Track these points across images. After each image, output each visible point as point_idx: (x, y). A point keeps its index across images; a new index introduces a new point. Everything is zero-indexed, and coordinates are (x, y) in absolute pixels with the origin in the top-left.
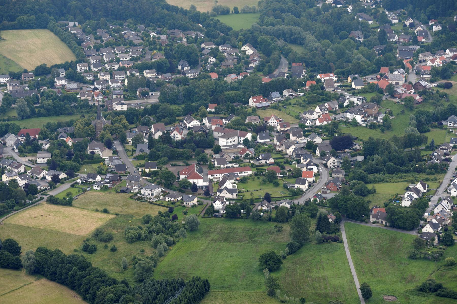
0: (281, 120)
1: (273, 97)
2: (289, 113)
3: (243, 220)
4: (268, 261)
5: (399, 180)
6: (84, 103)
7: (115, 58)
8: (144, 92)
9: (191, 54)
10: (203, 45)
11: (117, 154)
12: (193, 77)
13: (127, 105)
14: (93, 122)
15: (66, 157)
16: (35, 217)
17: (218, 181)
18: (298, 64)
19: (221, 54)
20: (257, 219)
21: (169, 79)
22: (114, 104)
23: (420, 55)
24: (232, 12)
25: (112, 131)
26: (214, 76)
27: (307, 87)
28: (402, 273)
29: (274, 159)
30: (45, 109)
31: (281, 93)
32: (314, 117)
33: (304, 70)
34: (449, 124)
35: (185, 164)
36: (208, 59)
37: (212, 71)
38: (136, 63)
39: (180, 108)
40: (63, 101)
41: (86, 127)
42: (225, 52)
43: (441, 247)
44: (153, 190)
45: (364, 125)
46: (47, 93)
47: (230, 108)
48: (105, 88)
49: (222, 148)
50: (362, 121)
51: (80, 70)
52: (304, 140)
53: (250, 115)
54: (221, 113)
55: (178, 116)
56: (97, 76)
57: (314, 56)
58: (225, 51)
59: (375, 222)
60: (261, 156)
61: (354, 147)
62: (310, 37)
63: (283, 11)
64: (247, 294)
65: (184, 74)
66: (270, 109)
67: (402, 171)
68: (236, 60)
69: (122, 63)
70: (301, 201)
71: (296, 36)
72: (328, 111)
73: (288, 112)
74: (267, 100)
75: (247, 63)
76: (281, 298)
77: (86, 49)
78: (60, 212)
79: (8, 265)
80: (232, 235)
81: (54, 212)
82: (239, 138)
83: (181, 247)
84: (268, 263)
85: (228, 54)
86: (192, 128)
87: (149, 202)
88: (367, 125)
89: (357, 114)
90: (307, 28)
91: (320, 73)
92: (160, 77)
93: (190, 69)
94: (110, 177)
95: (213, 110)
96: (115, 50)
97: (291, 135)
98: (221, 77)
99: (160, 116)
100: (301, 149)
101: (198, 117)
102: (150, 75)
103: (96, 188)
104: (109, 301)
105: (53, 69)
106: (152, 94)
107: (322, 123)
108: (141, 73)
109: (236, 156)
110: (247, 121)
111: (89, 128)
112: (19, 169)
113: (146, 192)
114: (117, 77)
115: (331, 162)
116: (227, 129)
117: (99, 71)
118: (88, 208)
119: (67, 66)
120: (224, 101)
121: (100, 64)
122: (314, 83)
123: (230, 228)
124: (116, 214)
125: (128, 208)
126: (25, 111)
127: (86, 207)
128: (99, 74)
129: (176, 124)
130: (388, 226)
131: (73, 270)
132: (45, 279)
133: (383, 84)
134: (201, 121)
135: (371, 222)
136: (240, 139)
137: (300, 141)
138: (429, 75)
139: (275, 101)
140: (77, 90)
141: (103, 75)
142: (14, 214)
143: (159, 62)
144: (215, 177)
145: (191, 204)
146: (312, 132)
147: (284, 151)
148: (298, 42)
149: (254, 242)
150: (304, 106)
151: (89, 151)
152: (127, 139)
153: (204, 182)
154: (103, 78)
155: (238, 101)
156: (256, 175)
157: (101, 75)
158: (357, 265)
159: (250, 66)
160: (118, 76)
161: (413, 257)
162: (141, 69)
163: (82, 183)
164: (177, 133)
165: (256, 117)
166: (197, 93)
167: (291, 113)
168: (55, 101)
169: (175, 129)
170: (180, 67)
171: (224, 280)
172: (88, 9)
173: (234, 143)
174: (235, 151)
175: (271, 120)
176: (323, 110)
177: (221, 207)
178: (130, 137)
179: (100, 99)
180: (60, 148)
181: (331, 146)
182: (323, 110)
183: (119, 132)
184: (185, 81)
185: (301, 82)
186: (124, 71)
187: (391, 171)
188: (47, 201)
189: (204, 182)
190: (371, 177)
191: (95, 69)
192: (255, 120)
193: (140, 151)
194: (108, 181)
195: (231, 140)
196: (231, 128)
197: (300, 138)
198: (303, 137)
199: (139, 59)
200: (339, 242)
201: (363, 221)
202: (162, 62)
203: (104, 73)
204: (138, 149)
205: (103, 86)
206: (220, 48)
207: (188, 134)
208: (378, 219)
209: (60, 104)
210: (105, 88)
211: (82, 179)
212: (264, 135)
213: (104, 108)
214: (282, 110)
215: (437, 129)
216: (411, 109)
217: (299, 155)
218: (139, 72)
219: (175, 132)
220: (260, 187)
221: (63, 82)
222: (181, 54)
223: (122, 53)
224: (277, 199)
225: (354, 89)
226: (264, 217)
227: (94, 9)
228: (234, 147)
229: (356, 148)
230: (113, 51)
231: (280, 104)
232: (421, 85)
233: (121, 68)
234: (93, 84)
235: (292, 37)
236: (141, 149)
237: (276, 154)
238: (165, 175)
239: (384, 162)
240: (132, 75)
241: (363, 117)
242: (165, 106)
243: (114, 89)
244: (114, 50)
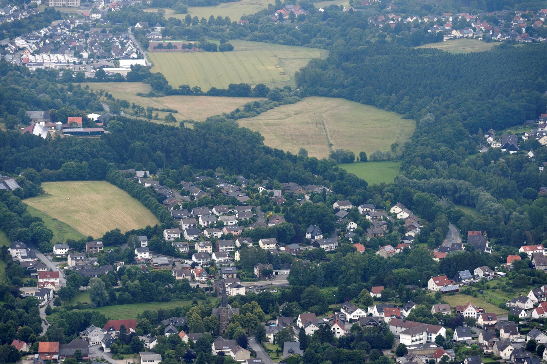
0: (481, 310)
1: (462, 277)
2: (490, 300)
6: (183, 285)
7: (215, 222)
8: (266, 269)
9: (324, 217)
10: (336, 205)
11: (255, 356)
12: (329, 250)
13: (244, 288)
14: (214, 310)
15: (184, 359)
18: (476, 233)
19: (363, 217)
21: (296, 252)
22: (226, 286)
24: (358, 159)
25: (243, 323)
26: (361, 248)
27: (509, 264)
30: (129, 293)
31: (472, 273)
32: (527, 307)
33: (488, 242)
36: (347, 224)
37: (356, 241)
38: (246, 229)
39: (330, 292)
40: (153, 281)
41: (206, 317)
42: (368, 215)
46: (129, 269)
47: (405, 292)
48: (208, 265)
49: (408, 348)
51: (169, 239)
52: (521, 338)
53: (433, 303)
54: (389, 300)
55: (330, 303)
56: (194, 247)
57: (497, 221)
58: (368, 213)
60: (466, 360)
62: (485, 195)
63: (435, 158)
65: (317, 244)
66: (460, 295)
68: (386, 226)
69: (227, 229)
71: (462, 193)
72: (545, 298)
73: (487, 298)
74: (454, 282)
75: (403, 231)
77: (172, 208)
82: (428, 335)
85: (373, 217)
86: (355, 320)
90: (478, 182)
91: (523, 245)
92: (282, 249)
93: (324, 238)
95: (379, 296)
96: (214, 210)
97: (502, 332)
98: (370, 250)
99: (304, 303)
100: (523, 350)
101: (361, 305)
102: (268, 246)
105: (131, 236)
106: (277, 273)
107: (541, 315)
108: (256, 243)
110: (433, 311)
111: (210, 318)
114: (222, 248)
116: (410, 322)
117: (195, 240)
119: (149, 233)
120: (392, 284)
121: (196, 230)
122: (519, 258)
126: (102, 295)
128: (196, 244)
129: (330, 314)
134: (366, 311)
136: (429, 336)
137: (515, 340)
139: (464, 284)
140: (167, 267)
141: (203, 245)
143: (280, 228)
146: (533, 328)
147: (496, 354)
148: (465, 202)
150: (510, 291)
151: (215, 352)
152: (267, 334)
154: (203, 249)
155: (412, 283)
157: (200, 245)
159: (407, 235)
160: (224, 248)
162: (256, 237)
164: (339, 327)
165: (446, 305)
166: (342, 272)
167: (492, 301)
168: (144, 282)
169: (334, 320)
170: (308, 236)
172: (159, 153)
173: (421, 342)
174: (426, 352)
175: (467, 309)
176: (539, 297)
178: (270, 332)
180: (174, 346)
182: (539, 297)
184: (320, 255)
185: (497, 257)
186: (231, 240)
191: (189, 238)
192: (445, 310)
193: (289, 352)
195: (417, 337)
196: (415, 320)
197: (514, 336)
198: (519, 335)
199: (250, 223)
202: (285, 228)
203: (204, 243)
206: (360, 209)
207: (352, 329)
209: (150, 285)
210: (208, 265)
212: (464, 330)
213: (212, 292)
214: (478, 296)
217: (521, 359)
218: (254, 241)
219: (336, 326)
221: (147, 255)
222: (310, 217)
223: (224, 215)
227: (167, 152)
228: (424, 347)
230: (210, 212)
231: (473, 288)
233: (227, 236)
234: (190, 258)
235: (457, 195)
236: (291, 349)
237: (485, 357)
240: (244, 246)
242: (312, 289)
243: (221, 266)
244: (212, 211)
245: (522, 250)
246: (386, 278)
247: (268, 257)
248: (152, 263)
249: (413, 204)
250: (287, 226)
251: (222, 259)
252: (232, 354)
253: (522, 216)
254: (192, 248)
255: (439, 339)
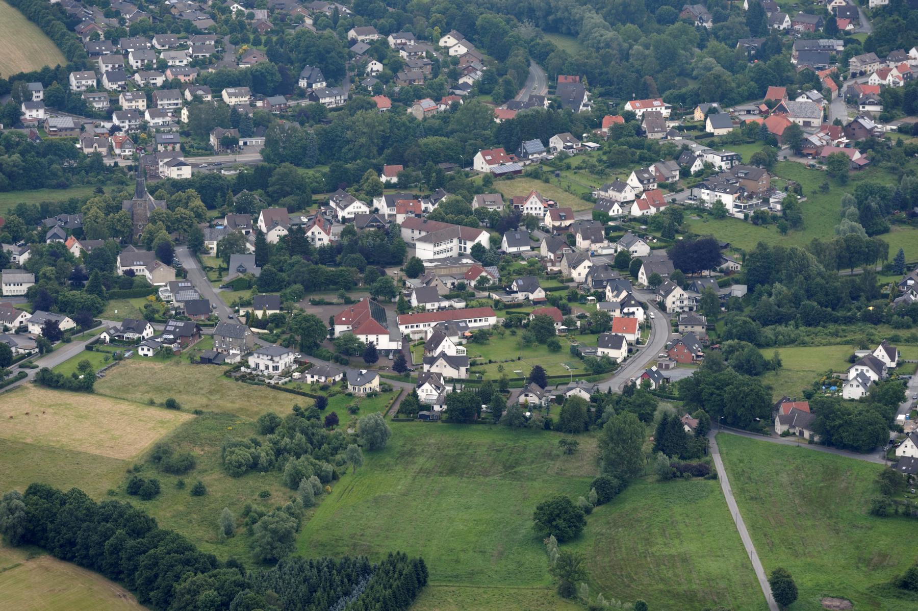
0: (552, 203)
1: (529, 151)
2: (569, 187)
3: (486, 427)
4: (554, 520)
5: (832, 340)
6: (92, 163)
7: (155, 61)
8: (228, 137)
9: (329, 52)
10: (352, 34)
11: (185, 277)
12: (334, 106)
13: (190, 167)
14: (126, 204)
15: (70, 282)
16: (11, 417)
17: (421, 339)
19: (394, 54)
21: (281, 110)
22: (161, 164)
23: (853, 60)
25: (169, 224)
26: (384, 103)
27: (605, 130)
28: (857, 548)
29: (546, 290)
31: (546, 143)
32: (625, 198)
33: (587, 93)
35: (342, 301)
36: (365, 65)
37: (378, 92)
39: (317, 175)
40: (44, 156)
41: (112, 215)
42: (403, 49)
44: (276, 359)
45: (741, 216)
46: (7, 137)
47: (434, 174)
48: (137, 129)
49: (425, 264)
50: (736, 206)
51: (78, 87)
53: (479, 191)
54: (411, 187)
55: (315, 192)
56: (118, 100)
57: (606, 60)
58: (403, 47)
59: (785, 434)
60: (514, 283)
61: (724, 266)
62: (592, 18)
64: (512, 591)
65: (314, 97)
66: (523, 179)
67: (836, 321)
68: (429, 67)
69: (172, 71)
70: (614, 385)
71: (559, 14)
72: (656, 185)
73: (564, 184)
74: (516, 158)
75: (455, 75)
77: (88, 39)
78: (67, 406)
80: (464, 460)
81: (53, 405)
82: (460, 243)
83: (350, 487)
84: (554, 523)
85: (410, 53)
86: (350, 220)
87: (269, 385)
88: (746, 216)
89: (725, 192)
91: (631, 99)
92: (259, 104)
93: (327, 86)
94: (176, 327)
95: (394, 180)
96: (154, 41)
97: (579, 238)
98: (399, 106)
99: (274, 192)
100: (606, 267)
101: (363, 196)
102: (237, 100)
103: (145, 352)
104: (206, 606)
105: (16, 83)
106: (245, 143)
107: (645, 212)
108: (217, 95)
109: (459, 284)
110: (475, 205)
111: (117, 216)
114: (163, 103)
115: (674, 299)
116: (434, 222)
117: (120, 89)
118: (129, 396)
119: (46, 77)
120: (417, 160)
121: (123, 73)
122: (621, 120)
124: (196, 412)
127: (125, 396)
128: (121, 96)
129: (313, 210)
132: (48, 557)
133: (776, 124)
134: (370, 204)
135: (777, 433)
136: (463, 245)
137: (599, 251)
138: (876, 104)
139: (532, 161)
140: (72, 132)
141: (131, 97)
143: (257, 71)
144: (415, 329)
146: (626, 231)
147: (565, 272)
148: (564, 29)
149: (517, 476)
150: (601, 173)
151: (120, 271)
152: (206, 242)
153: (391, 340)
154: (131, 104)
155: (449, 159)
156: (507, 325)
157: (127, 98)
158: (754, 529)
159: (461, 81)
160: (166, 102)
161: (879, 512)
162: (217, 85)
163: (112, 341)
164: (320, 230)
165: (496, 195)
166: (348, 142)
167: (572, 188)
168: (28, 157)
169: (313, 221)
170: (303, 83)
171: (457, 561)
173: (449, 254)
174: (455, 271)
176: (646, 182)
177: (435, 398)
178: (211, 239)
180: (55, 261)
181: (672, 261)
182: (646, 182)
183: (185, 227)
184: (318, 114)
185: (588, 119)
186: (178, 90)
187: (811, 320)
188: (35, 381)
189: (391, 340)
191: (111, 86)
192: (494, 203)
193: (238, 271)
194: (172, 337)
195: (443, 247)
196: (443, 220)
197: (598, 245)
198: (606, 243)
199: (211, 63)
200: (709, 479)
201: (759, 431)
202: (263, 71)
203: (132, 95)
204: (233, 265)
206: (391, 40)
207: (343, 234)
208: (794, 427)
209: (38, 162)
210: (137, 129)
211: (112, 332)
212: (518, 236)
214: (551, 180)
215: (904, 227)
216: (843, 181)
217: (602, 281)
218: (213, 92)
219: (316, 229)
221: (40, 114)
222: (306, 52)
223: (171, 48)
224: (558, 381)
225: (712, 135)
226: (534, 421)
228: (451, 263)
229: (728, 268)
230: (149, 45)
231: (546, 168)
232: (862, 127)
233: (171, 83)
234: (109, 119)
235: (551, 18)
236: (241, 266)
237: (548, 279)
239: (796, 301)
240: (197, 99)
241: (739, 198)
242: (285, 170)
243: (158, 131)
244: (151, 43)
245: (628, 107)
246: (408, 152)
247: (234, 119)
248: (47, 126)
249: (476, 33)
250: (267, 68)
251: (159, 121)
252: (147, 274)
253: (647, 52)
254: (114, 102)
255: (478, 251)
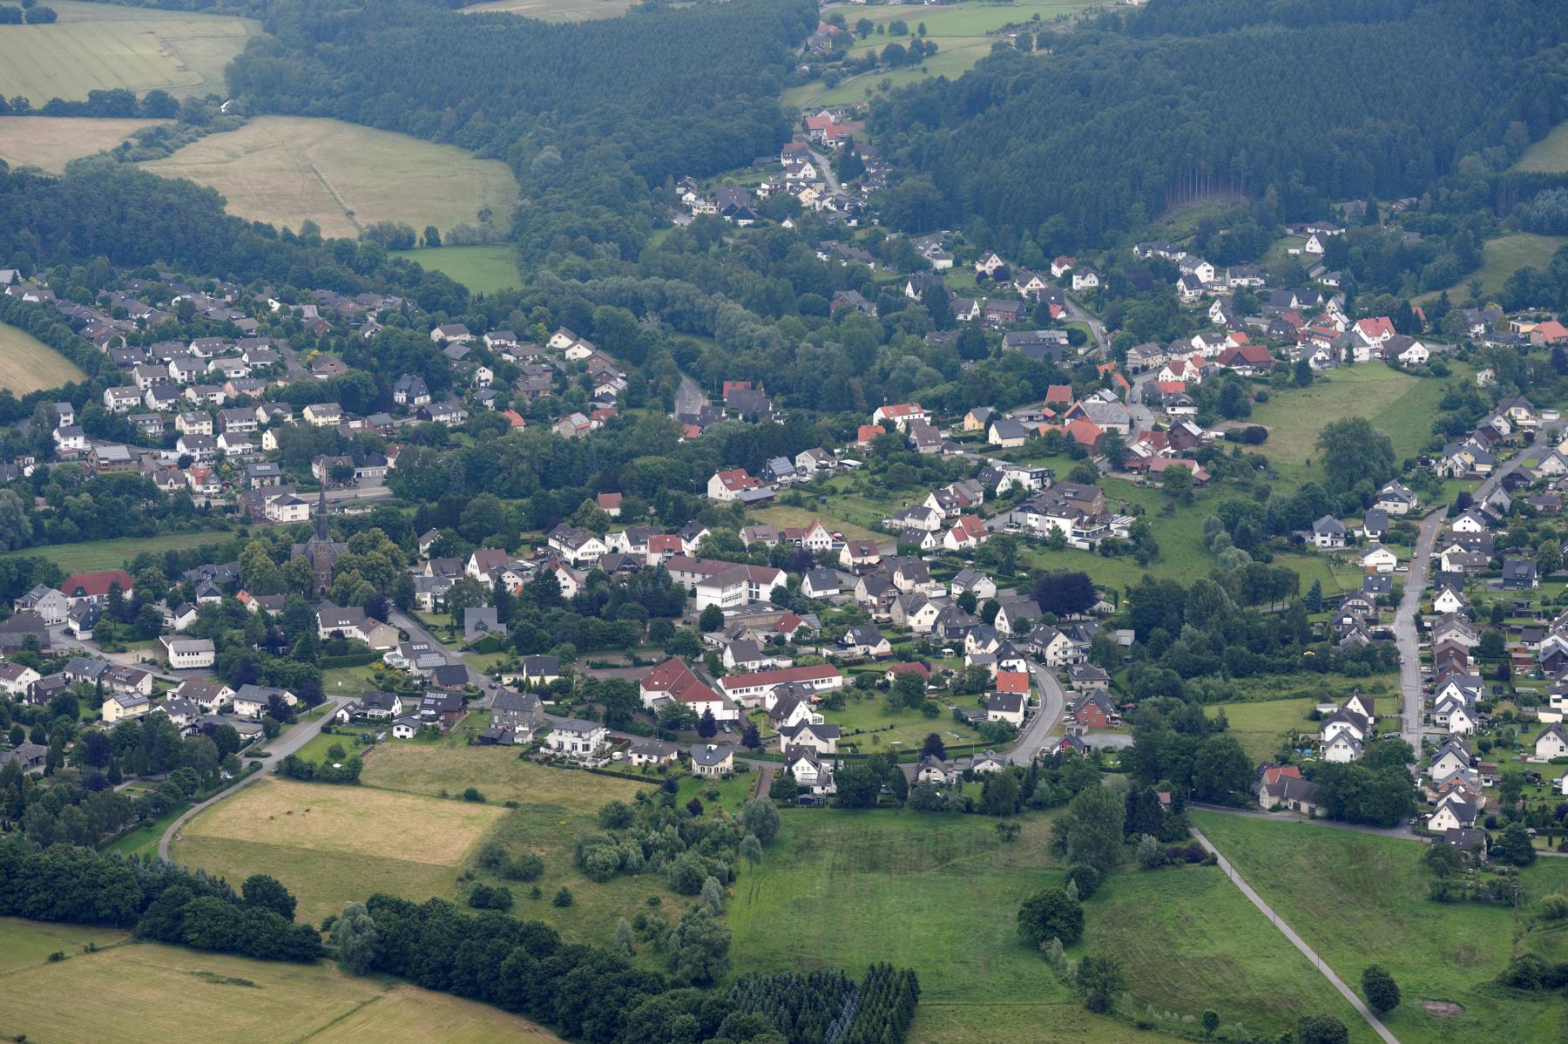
1: (777, 472)
3: (891, 812)
4: (1048, 919)
5: (1278, 694)
9: (430, 357)
10: (437, 334)
16: (272, 818)
17: (757, 706)
18: (741, 385)
20: (930, 805)
22: (268, 502)
23: (1133, 351)
24: (421, 241)
27: (862, 443)
28: (1434, 941)
29: (892, 642)
30: (71, 519)
34: (1318, 539)
35: (631, 662)
36: (473, 371)
38: (271, 385)
39: (510, 508)
43: (1505, 868)
44: (585, 736)
45: (1086, 546)
50: (1076, 534)
52: (936, 589)
59: (1275, 809)
61: (1096, 607)
63: (594, 237)
64: (1027, 1008)
67: (1272, 670)
68: (549, 375)
69: (234, 385)
70: (1022, 756)
71: (678, 306)
74: (762, 483)
75: (588, 384)
76: (1137, 1016)
77: (105, 346)
78: (335, 803)
79: (281, 951)
80: (881, 852)
81: (320, 801)
82: (751, 586)
83: (755, 890)
84: (1049, 923)
87: (585, 768)
88: (1092, 546)
89: (1060, 516)
90: (709, 282)
91: (882, 405)
94: (437, 700)
102: (325, 420)
103: (403, 732)
104: (682, 1035)
108: (299, 415)
109: (777, 637)
112: (139, 685)
113: (562, 739)
114: (234, 426)
115: (1056, 649)
116: (710, 562)
118: (410, 788)
121: (166, 388)
123: (866, 834)
124: (509, 805)
125: (531, 786)
126: (18, 526)
127: (403, 787)
130: (1320, 818)
131: (512, 955)
132: (410, 986)
133: (1086, 432)
135: (1263, 808)
138: (1190, 405)
139: (781, 484)
142: (202, 811)
143: (345, 382)
144: (745, 694)
145: (717, 770)
149: (957, 870)
153: (725, 708)
156: (859, 685)
158: (1292, 921)
159: (598, 392)
160: (237, 424)
161: (1441, 898)
162: (299, 398)
163: (353, 720)
166: (500, 470)
171: (940, 975)
172: (25, 232)
173: (738, 601)
175: (813, 534)
177: (815, 777)
179: (212, 490)
181: (1036, 603)
183: (383, 576)
187: (1240, 670)
188: (276, 773)
189: (725, 708)
190: (1194, 684)
193: (477, 629)
194: (433, 712)
195: (732, 592)
196: (719, 558)
197: (924, 585)
198: (933, 582)
200: (1206, 865)
201: (1240, 805)
204: (469, 622)
205: (205, 451)
208: (1286, 799)
209: (115, 503)
211: (350, 707)
213: (239, 515)
215: (1288, 555)
216: (1188, 501)
217: (958, 629)
218: (294, 410)
220: (887, 722)
221: (79, 443)
222: (400, 357)
223: (216, 356)
224: (961, 752)
225: (999, 447)
226: (954, 803)
227: (42, 230)
229: (1100, 610)
231: (804, 494)
232: (1188, 433)
234: (173, 447)
238: (612, 691)
239: (1216, 647)
241: (1078, 523)
243: (240, 461)
245: (879, 415)
246: (622, 476)
247: (327, 443)
248: (95, 459)
249: (593, 329)
250: (359, 378)
251: (238, 448)
252: (361, 635)
253: (819, 350)
254: (170, 425)
255: (778, 595)
